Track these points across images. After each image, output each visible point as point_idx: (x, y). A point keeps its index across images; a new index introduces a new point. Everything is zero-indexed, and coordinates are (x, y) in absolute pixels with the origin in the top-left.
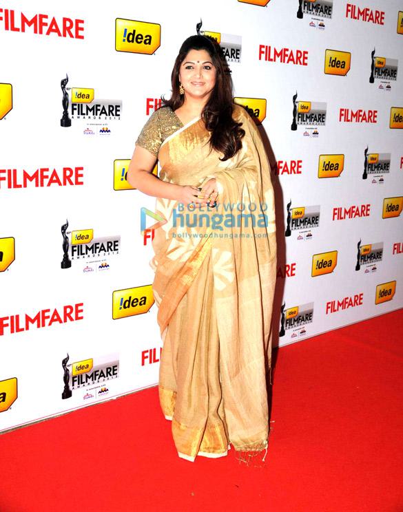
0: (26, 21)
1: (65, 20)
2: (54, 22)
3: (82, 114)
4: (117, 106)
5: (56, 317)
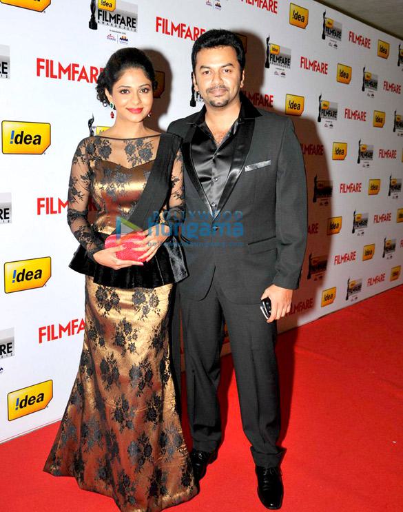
0: (63, 69)
1: (92, 68)
2: (83, 69)
5: (82, 326)
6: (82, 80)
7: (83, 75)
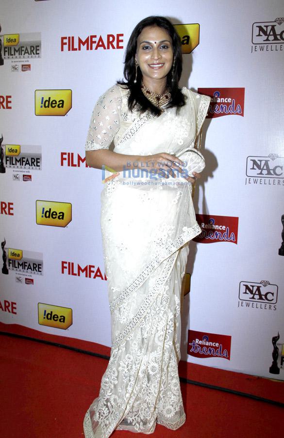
1: (109, 36)
2: (101, 39)
3: (13, 164)
4: (37, 159)
7: (101, 43)
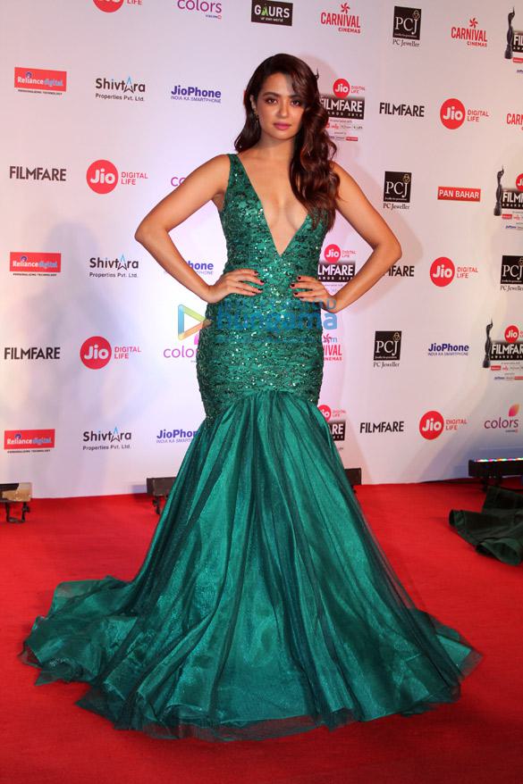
1: (53, 170)
2: (46, 172)
6: (45, 179)
